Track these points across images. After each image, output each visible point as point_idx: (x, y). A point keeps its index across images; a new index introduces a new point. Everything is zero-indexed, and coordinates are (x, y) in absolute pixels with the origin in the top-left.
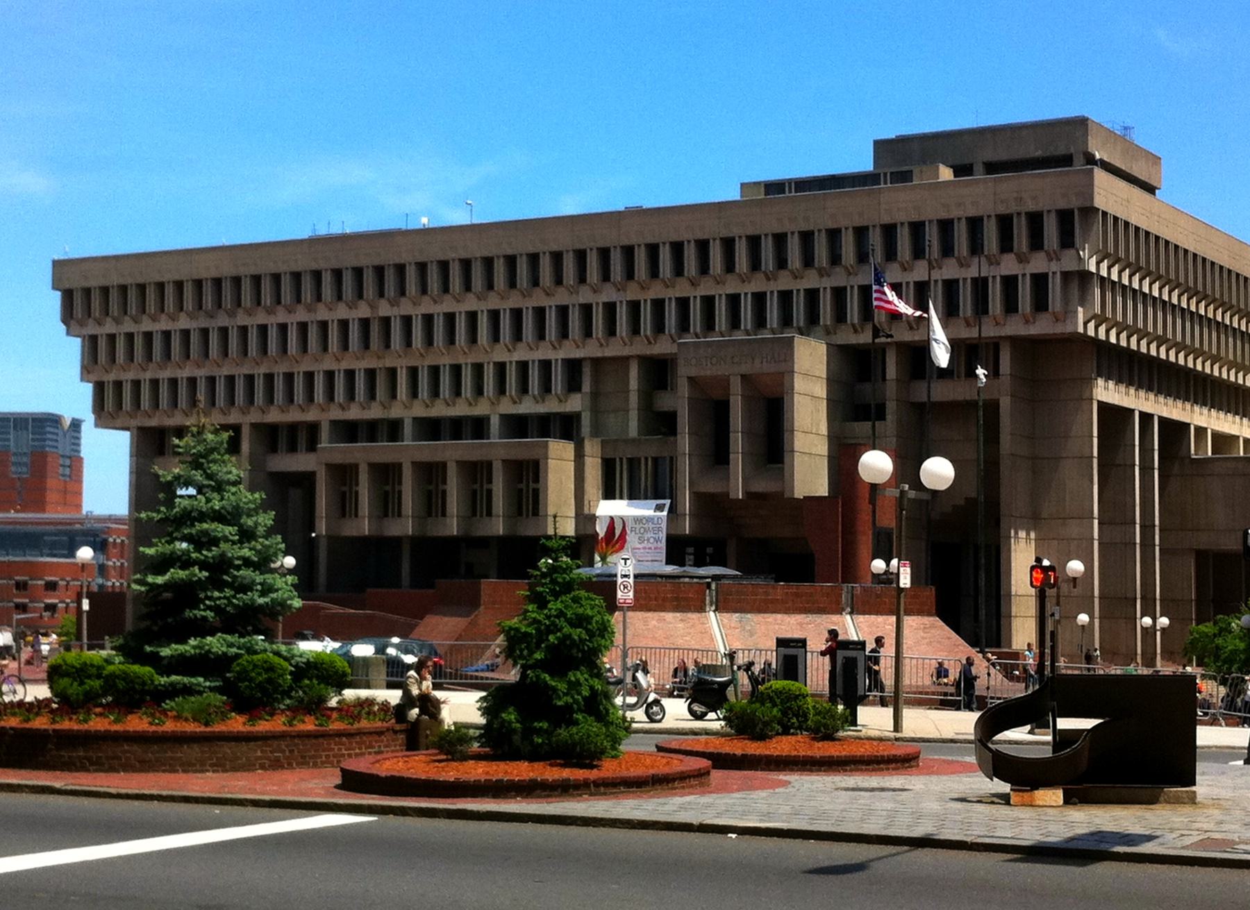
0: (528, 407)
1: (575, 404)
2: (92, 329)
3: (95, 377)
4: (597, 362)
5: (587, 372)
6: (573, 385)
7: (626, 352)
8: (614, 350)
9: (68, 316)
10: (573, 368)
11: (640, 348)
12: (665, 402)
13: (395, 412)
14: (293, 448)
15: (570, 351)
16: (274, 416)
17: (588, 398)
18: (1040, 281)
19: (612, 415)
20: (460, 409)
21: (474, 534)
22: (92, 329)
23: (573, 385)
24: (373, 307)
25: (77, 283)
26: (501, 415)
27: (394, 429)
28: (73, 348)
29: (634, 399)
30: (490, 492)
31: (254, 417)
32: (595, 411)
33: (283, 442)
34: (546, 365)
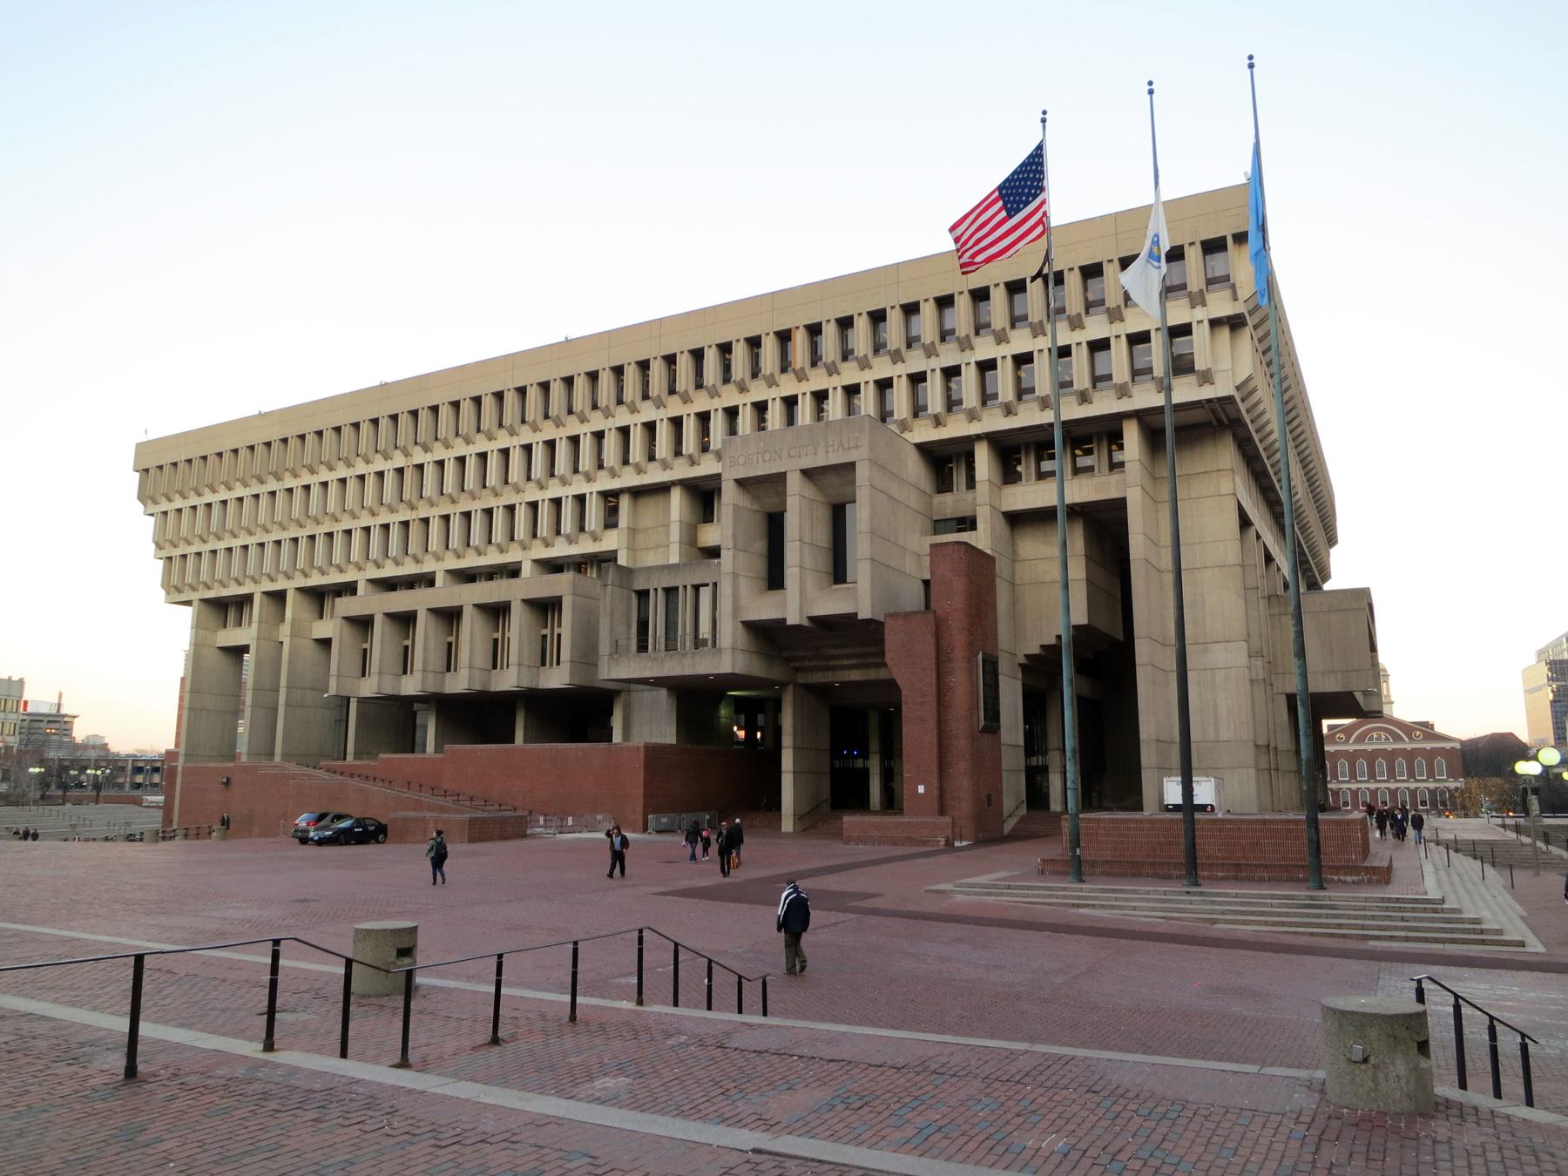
1: (611, 541)
3: (165, 554)
4: (637, 493)
5: (625, 503)
8: (655, 475)
10: (610, 498)
11: (682, 471)
12: (710, 535)
13: (428, 566)
17: (625, 537)
19: (652, 553)
20: (492, 558)
21: (447, 691)
22: (165, 506)
23: (611, 522)
26: (535, 561)
28: (147, 526)
29: (675, 532)
32: (632, 549)
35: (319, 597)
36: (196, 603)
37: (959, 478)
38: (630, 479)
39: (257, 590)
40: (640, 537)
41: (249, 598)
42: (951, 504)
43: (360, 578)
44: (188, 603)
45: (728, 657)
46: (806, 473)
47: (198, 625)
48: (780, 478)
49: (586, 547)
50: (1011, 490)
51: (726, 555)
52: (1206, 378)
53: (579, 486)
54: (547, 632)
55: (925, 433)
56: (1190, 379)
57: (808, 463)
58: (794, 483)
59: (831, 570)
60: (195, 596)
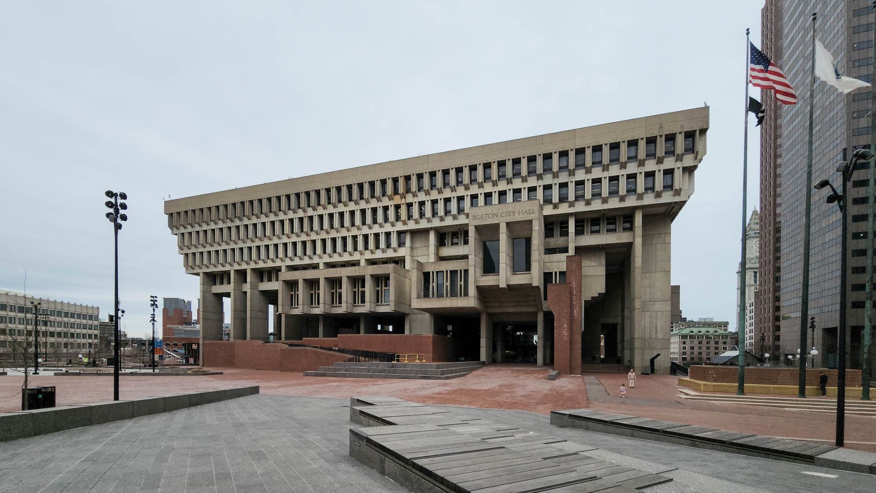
0: (379, 255)
1: (402, 252)
2: (182, 230)
4: (414, 233)
6: (401, 244)
7: (429, 225)
8: (423, 224)
9: (171, 226)
11: (436, 223)
14: (270, 280)
15: (400, 227)
16: (261, 265)
17: (409, 250)
18: (669, 172)
23: (401, 244)
24: (305, 211)
25: (174, 210)
27: (315, 267)
30: (363, 293)
31: (253, 266)
33: (265, 277)
34: (388, 234)
35: (262, 274)
36: (201, 274)
37: (557, 232)
38: (411, 225)
39: (232, 268)
40: (415, 251)
41: (228, 273)
42: (557, 241)
43: (283, 265)
44: (198, 274)
45: (470, 301)
46: (508, 224)
47: (204, 284)
48: (496, 226)
49: (390, 254)
50: (580, 237)
51: (472, 258)
52: (678, 192)
53: (388, 228)
54: (379, 289)
55: (549, 211)
56: (671, 193)
57: (510, 219)
58: (503, 229)
59: (511, 265)
60: (201, 271)
